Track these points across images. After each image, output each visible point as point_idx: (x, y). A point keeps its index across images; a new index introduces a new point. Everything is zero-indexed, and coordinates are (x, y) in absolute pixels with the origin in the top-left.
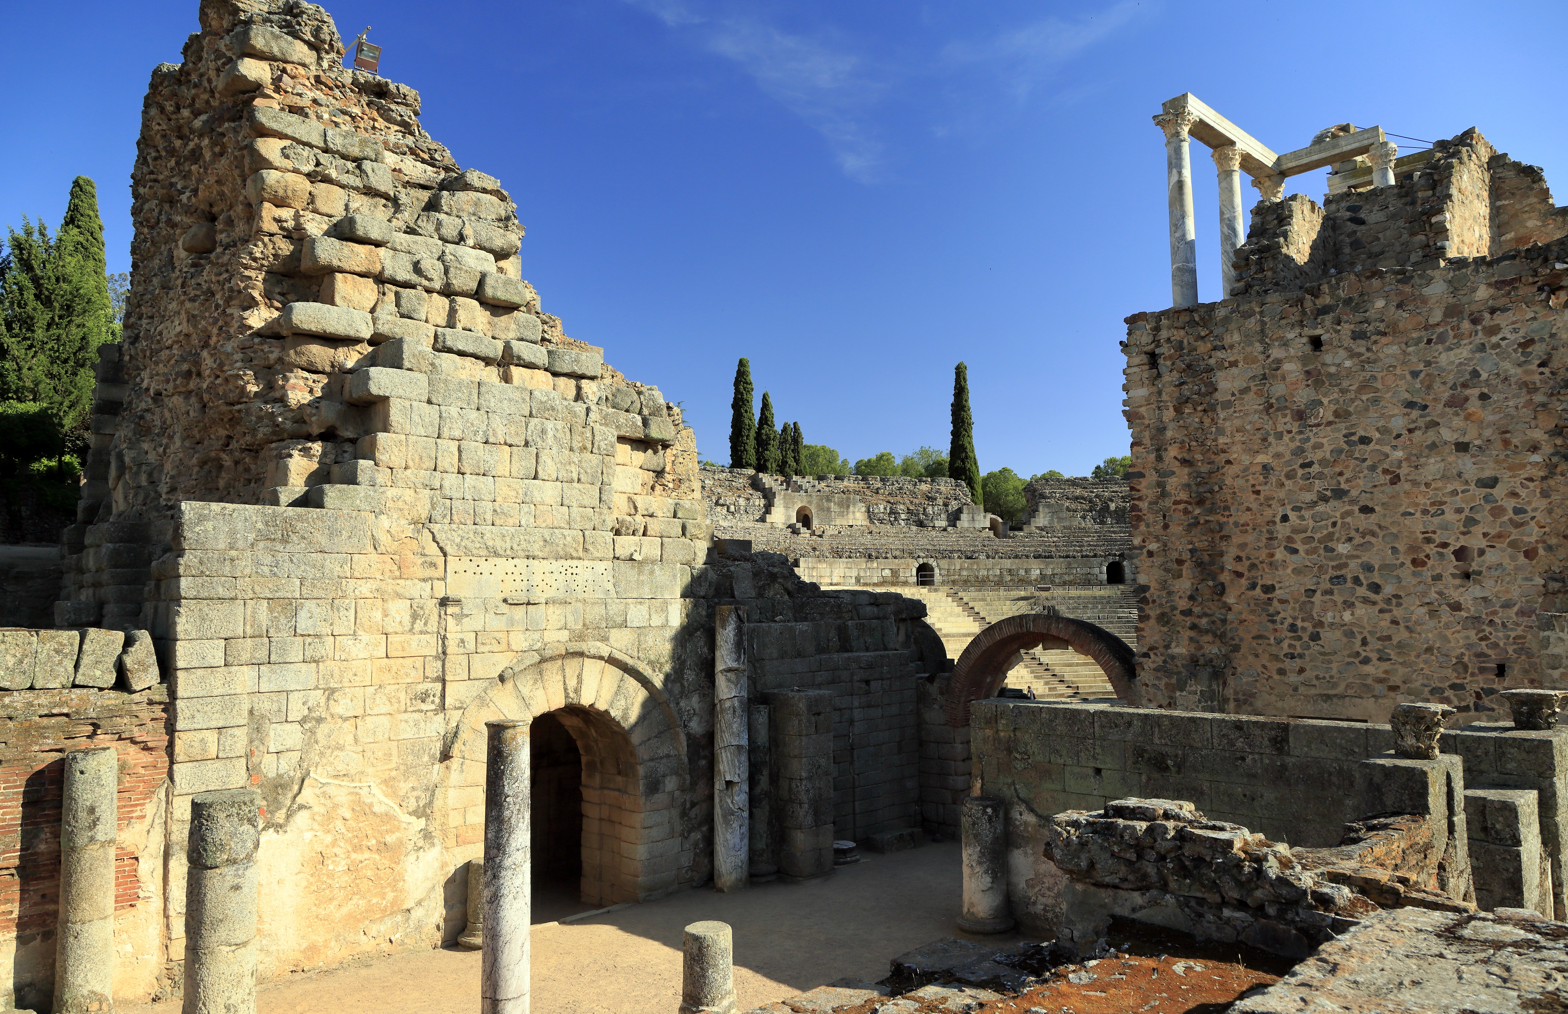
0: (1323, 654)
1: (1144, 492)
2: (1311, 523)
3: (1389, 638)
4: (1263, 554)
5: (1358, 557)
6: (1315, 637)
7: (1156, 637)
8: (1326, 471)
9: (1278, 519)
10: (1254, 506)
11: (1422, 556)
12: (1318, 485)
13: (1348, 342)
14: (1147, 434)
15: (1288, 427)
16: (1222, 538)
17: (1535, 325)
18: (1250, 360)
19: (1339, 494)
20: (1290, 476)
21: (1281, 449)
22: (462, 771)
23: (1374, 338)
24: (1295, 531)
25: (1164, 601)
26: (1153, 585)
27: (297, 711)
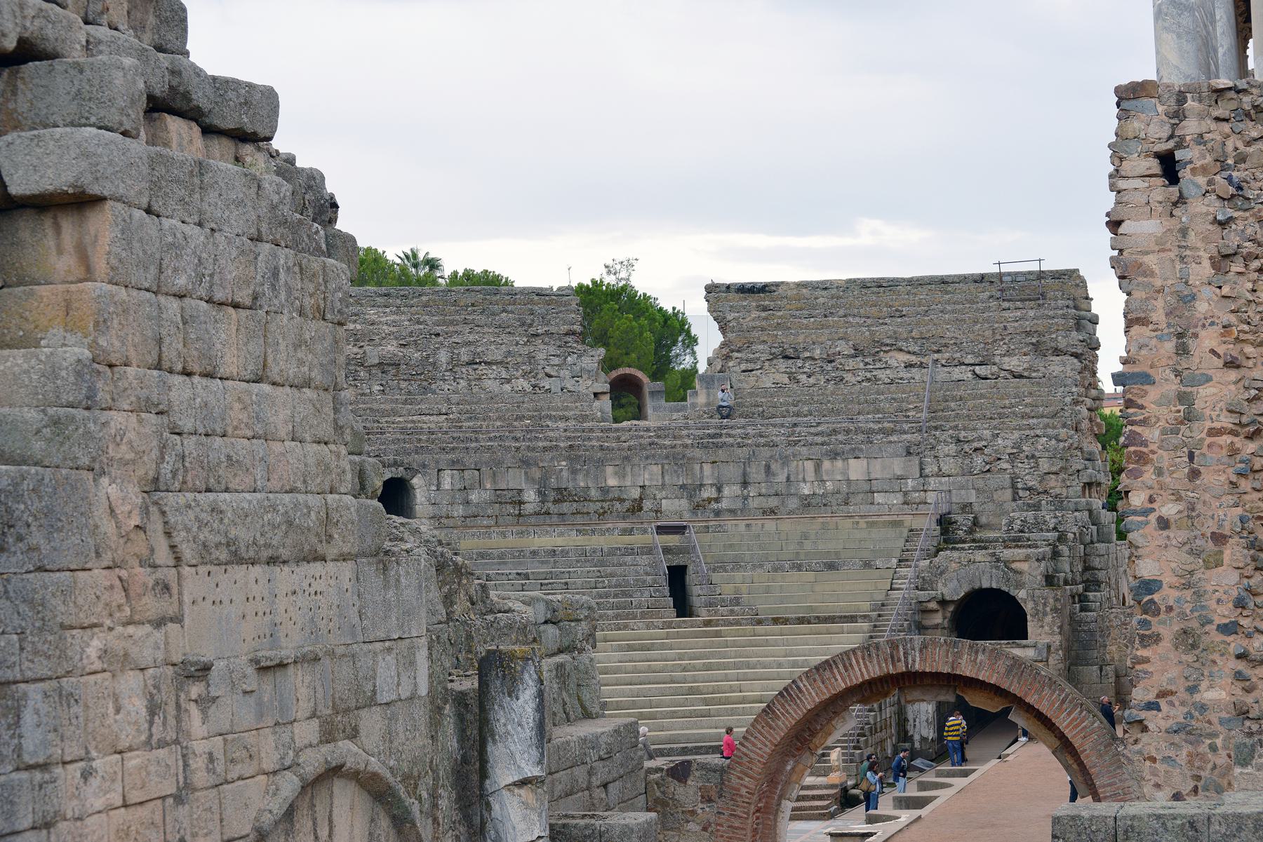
1: (1152, 409)
7: (1174, 672)
14: (1160, 303)
25: (1187, 608)
26: (1167, 579)
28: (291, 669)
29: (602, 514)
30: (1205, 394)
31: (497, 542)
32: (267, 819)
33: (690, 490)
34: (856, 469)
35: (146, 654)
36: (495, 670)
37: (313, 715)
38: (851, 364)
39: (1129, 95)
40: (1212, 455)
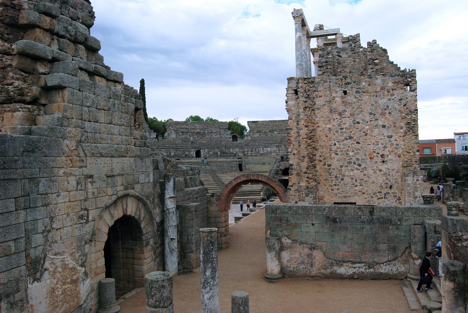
0: (344, 184)
2: (342, 146)
3: (363, 179)
4: (328, 155)
5: (354, 156)
6: (342, 179)
7: (295, 180)
8: (347, 131)
9: (333, 145)
10: (326, 140)
11: (372, 156)
12: (345, 135)
13: (354, 94)
14: (294, 116)
15: (337, 117)
16: (316, 150)
17: (403, 95)
18: (326, 96)
19: (351, 138)
20: (337, 132)
21: (335, 124)
22: (95, 246)
23: (362, 93)
24: (337, 148)
26: (295, 164)
27: (41, 228)
28: (116, 177)
29: (230, 156)
30: (301, 132)
31: (213, 160)
32: (108, 204)
33: (243, 152)
34: (269, 149)
35: (77, 173)
36: (166, 178)
37: (122, 185)
38: (269, 133)
39: (290, 79)
40: (303, 142)
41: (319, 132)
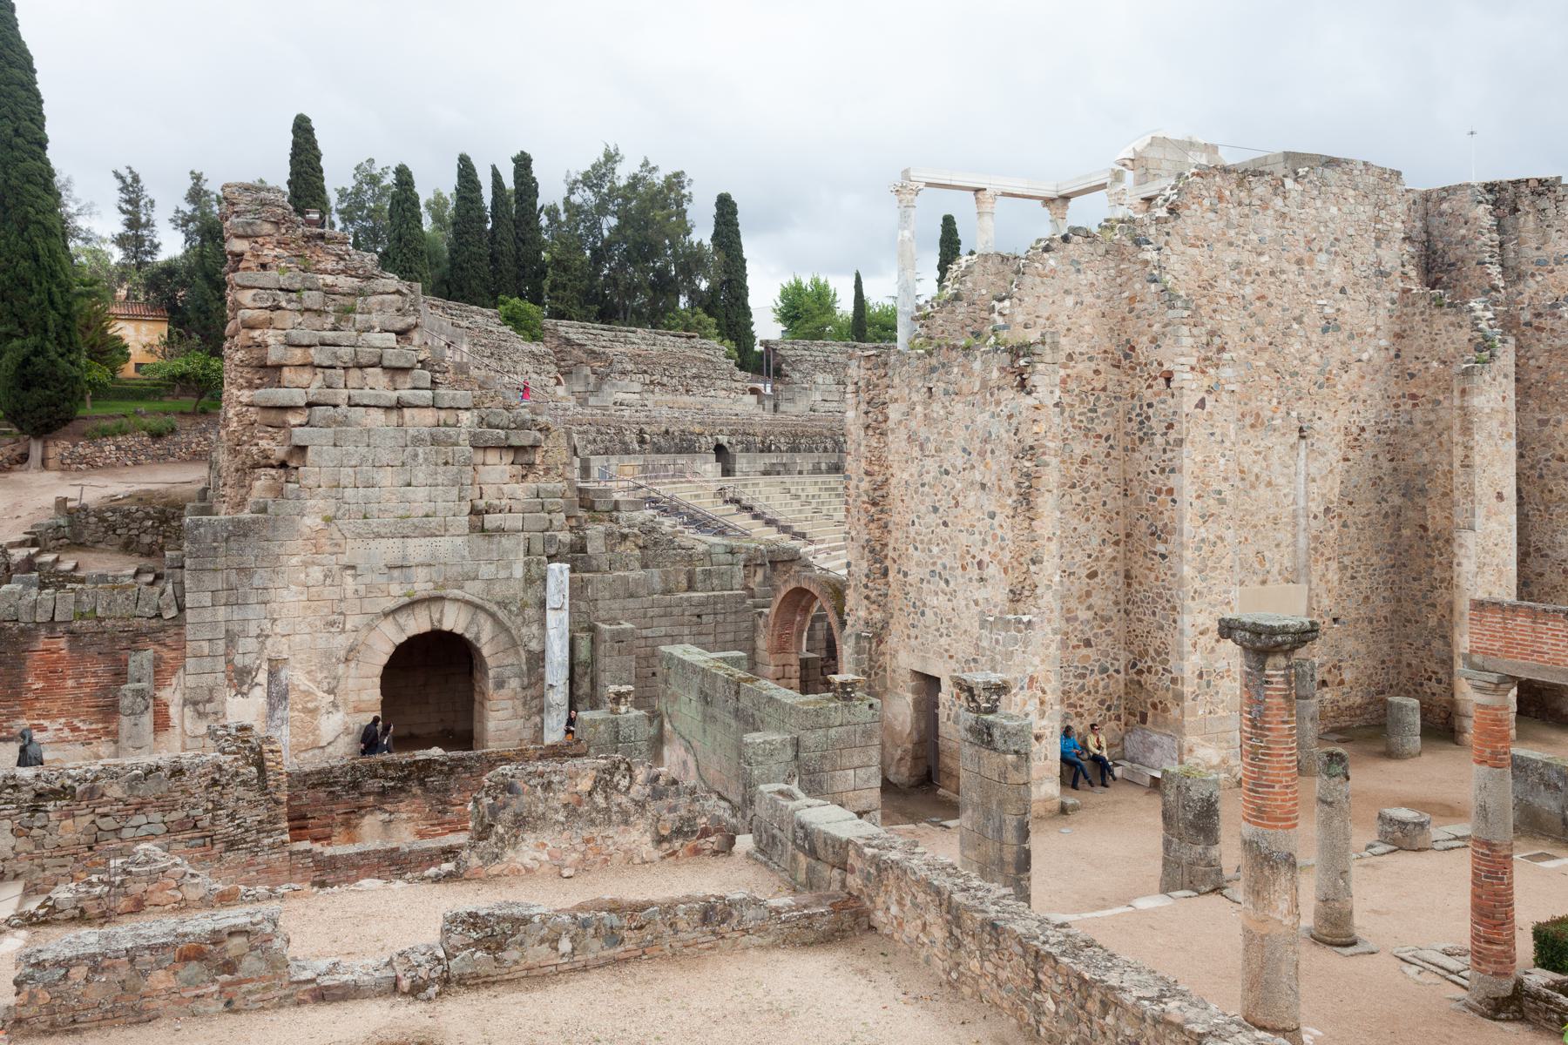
17: (1014, 403)
41: (895, 491)
